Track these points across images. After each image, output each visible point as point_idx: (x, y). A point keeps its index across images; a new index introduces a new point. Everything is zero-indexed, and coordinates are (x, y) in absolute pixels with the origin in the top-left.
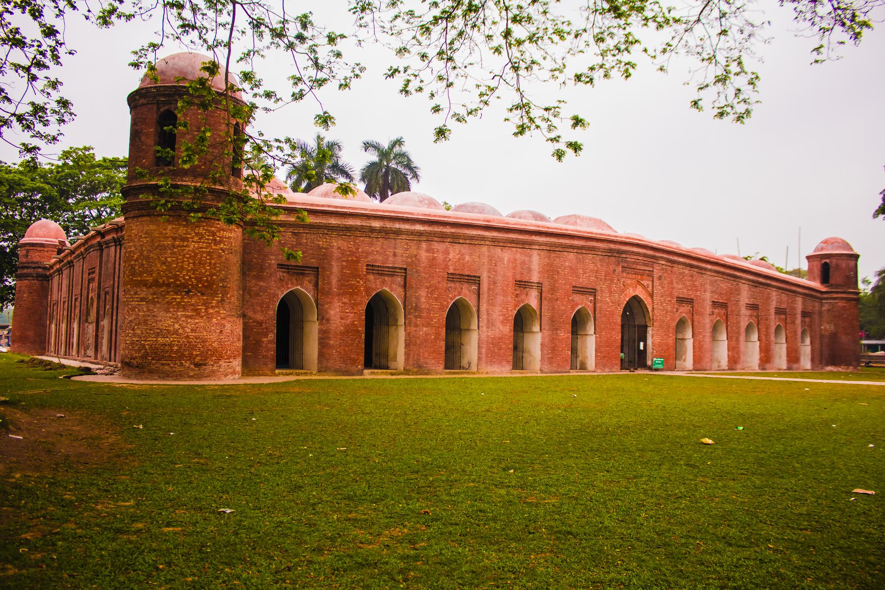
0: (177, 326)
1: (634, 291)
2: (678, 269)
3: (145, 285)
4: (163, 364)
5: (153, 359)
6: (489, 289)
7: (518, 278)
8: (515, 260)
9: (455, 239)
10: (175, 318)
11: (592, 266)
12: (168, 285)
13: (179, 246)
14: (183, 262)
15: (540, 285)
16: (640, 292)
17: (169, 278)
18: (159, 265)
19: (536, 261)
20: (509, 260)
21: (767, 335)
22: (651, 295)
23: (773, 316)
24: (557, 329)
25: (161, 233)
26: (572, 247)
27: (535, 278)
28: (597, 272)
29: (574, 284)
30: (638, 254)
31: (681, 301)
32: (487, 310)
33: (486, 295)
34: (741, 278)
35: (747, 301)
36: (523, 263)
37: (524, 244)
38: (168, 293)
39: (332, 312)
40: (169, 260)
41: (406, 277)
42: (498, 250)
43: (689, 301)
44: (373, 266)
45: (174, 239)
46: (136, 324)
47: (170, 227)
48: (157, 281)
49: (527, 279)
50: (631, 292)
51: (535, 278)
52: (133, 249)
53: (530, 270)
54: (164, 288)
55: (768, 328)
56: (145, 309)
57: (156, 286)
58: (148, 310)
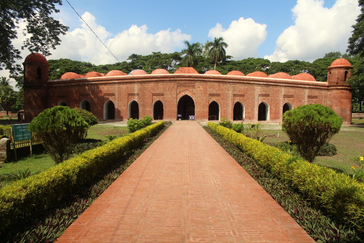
1: (185, 93)
2: (209, 84)
6: (118, 97)
7: (129, 93)
8: (128, 88)
9: (105, 84)
11: (162, 86)
15: (138, 94)
19: (136, 88)
20: (125, 88)
22: (194, 94)
23: (282, 98)
24: (145, 108)
26: (153, 81)
27: (136, 92)
28: (164, 88)
29: (153, 93)
31: (212, 95)
32: (118, 103)
33: (117, 99)
34: (254, 84)
35: (259, 93)
36: (131, 88)
37: (131, 83)
42: (121, 85)
43: (218, 95)
49: (133, 93)
50: (183, 94)
51: (136, 92)
53: (134, 90)
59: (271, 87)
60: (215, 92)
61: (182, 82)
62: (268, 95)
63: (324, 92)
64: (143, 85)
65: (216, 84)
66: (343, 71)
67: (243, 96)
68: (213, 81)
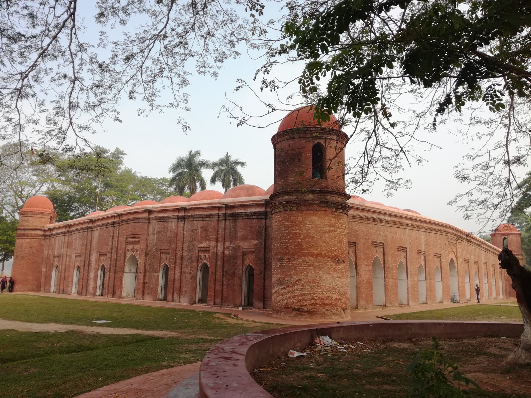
0: (334, 284)
3: (312, 256)
4: (327, 310)
5: (320, 306)
10: (333, 278)
12: (328, 256)
13: (332, 231)
14: (335, 241)
17: (328, 251)
18: (321, 243)
25: (321, 222)
38: (328, 261)
39: (362, 271)
40: (327, 239)
41: (384, 248)
44: (375, 242)
45: (330, 226)
46: (305, 282)
47: (327, 218)
48: (321, 254)
52: (298, 231)
54: (325, 259)
56: (313, 272)
57: (320, 257)
58: (315, 273)
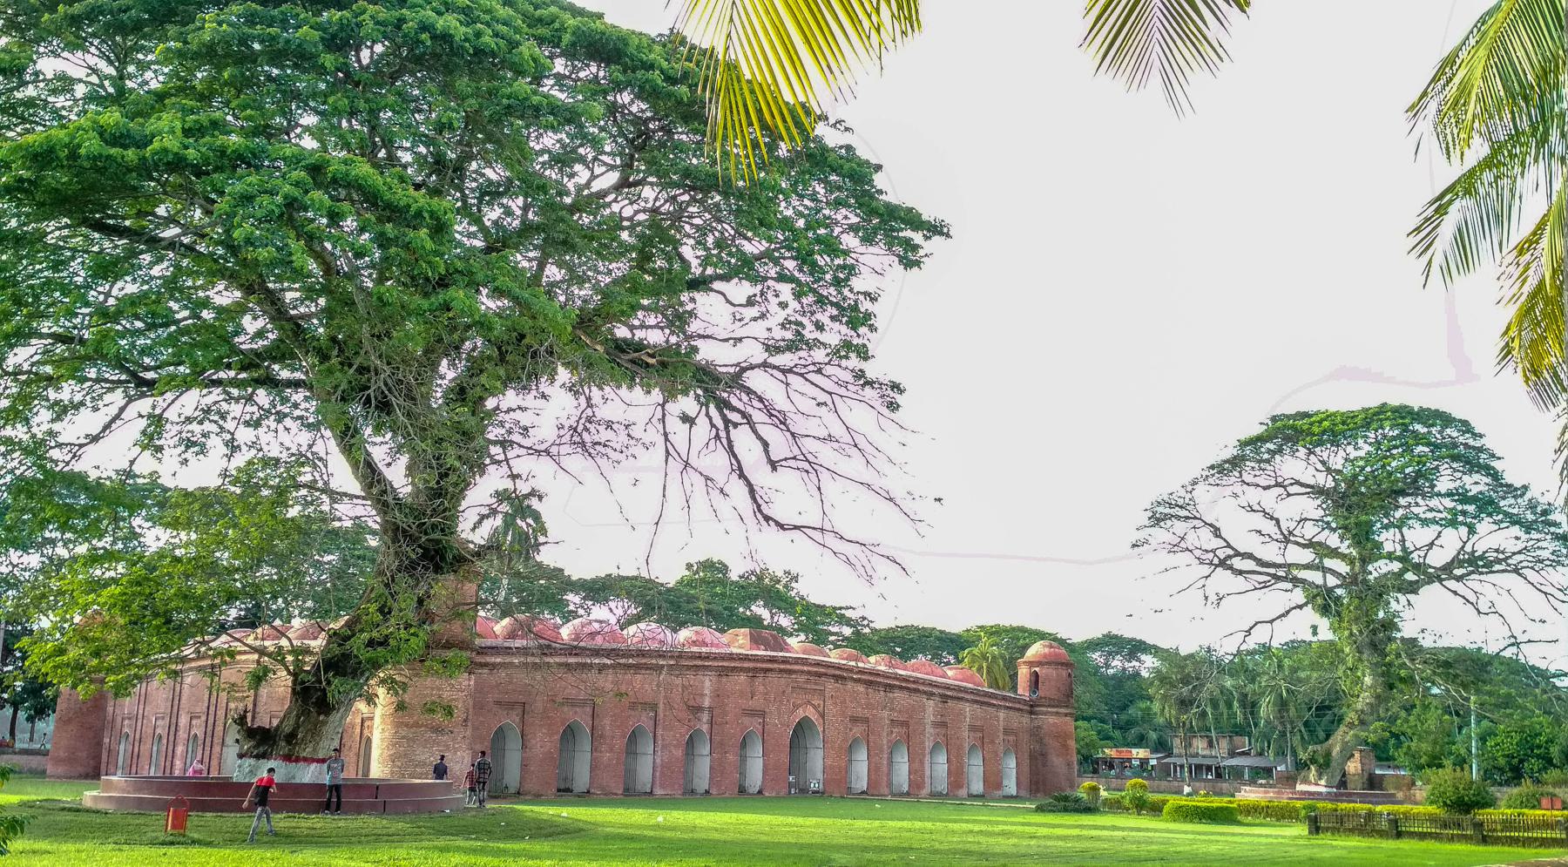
2: (850, 685)
11: (761, 688)
16: (811, 713)
21: (959, 757)
22: (823, 716)
30: (809, 673)
31: (855, 720)
43: (866, 720)
50: (800, 713)
55: (960, 748)
59: (950, 703)
60: (860, 712)
61: (802, 678)
62: (943, 725)
63: (1026, 719)
64: (724, 679)
65: (861, 688)
66: (1064, 673)
67: (905, 724)
68: (858, 681)
